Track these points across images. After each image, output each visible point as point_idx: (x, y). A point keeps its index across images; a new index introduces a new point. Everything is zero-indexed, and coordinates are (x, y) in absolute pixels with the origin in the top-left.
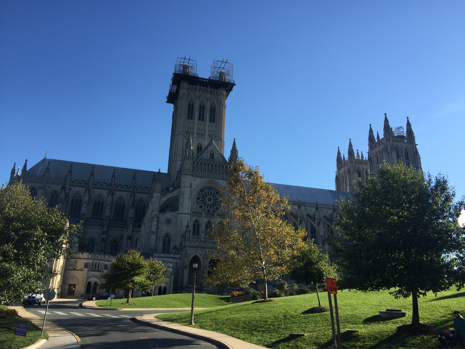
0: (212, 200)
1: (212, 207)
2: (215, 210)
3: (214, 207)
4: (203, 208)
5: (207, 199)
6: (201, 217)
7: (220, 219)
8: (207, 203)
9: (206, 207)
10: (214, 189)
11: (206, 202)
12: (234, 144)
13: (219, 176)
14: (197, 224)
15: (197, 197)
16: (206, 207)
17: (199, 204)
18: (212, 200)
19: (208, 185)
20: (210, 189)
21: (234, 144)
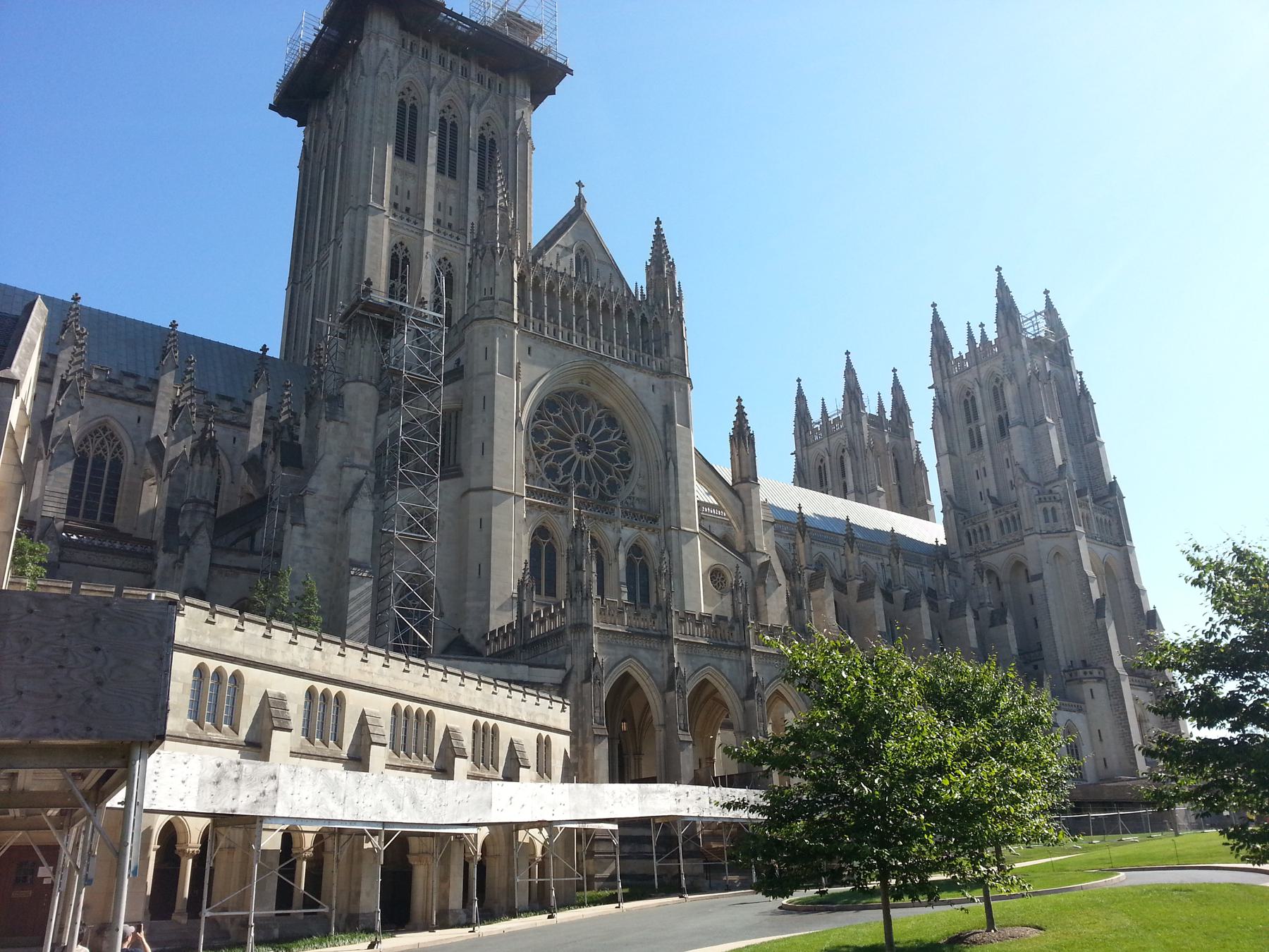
0: (595, 449)
1: (595, 480)
2: (608, 493)
3: (601, 478)
4: (562, 477)
5: (573, 442)
6: (562, 512)
7: (635, 530)
8: (574, 458)
9: (572, 473)
10: (600, 406)
11: (571, 453)
12: (659, 239)
13: (621, 348)
14: (544, 544)
15: (535, 429)
16: (572, 473)
17: (544, 458)
18: (595, 449)
19: (575, 383)
20: (583, 400)
21: (659, 239)
